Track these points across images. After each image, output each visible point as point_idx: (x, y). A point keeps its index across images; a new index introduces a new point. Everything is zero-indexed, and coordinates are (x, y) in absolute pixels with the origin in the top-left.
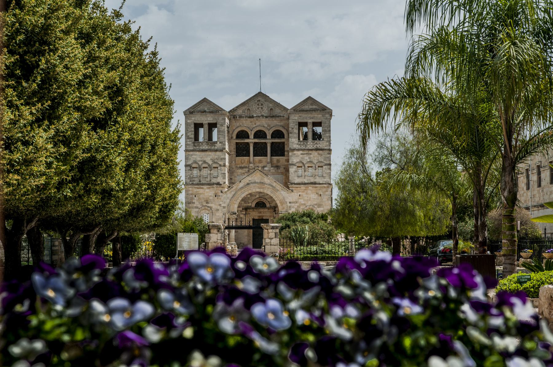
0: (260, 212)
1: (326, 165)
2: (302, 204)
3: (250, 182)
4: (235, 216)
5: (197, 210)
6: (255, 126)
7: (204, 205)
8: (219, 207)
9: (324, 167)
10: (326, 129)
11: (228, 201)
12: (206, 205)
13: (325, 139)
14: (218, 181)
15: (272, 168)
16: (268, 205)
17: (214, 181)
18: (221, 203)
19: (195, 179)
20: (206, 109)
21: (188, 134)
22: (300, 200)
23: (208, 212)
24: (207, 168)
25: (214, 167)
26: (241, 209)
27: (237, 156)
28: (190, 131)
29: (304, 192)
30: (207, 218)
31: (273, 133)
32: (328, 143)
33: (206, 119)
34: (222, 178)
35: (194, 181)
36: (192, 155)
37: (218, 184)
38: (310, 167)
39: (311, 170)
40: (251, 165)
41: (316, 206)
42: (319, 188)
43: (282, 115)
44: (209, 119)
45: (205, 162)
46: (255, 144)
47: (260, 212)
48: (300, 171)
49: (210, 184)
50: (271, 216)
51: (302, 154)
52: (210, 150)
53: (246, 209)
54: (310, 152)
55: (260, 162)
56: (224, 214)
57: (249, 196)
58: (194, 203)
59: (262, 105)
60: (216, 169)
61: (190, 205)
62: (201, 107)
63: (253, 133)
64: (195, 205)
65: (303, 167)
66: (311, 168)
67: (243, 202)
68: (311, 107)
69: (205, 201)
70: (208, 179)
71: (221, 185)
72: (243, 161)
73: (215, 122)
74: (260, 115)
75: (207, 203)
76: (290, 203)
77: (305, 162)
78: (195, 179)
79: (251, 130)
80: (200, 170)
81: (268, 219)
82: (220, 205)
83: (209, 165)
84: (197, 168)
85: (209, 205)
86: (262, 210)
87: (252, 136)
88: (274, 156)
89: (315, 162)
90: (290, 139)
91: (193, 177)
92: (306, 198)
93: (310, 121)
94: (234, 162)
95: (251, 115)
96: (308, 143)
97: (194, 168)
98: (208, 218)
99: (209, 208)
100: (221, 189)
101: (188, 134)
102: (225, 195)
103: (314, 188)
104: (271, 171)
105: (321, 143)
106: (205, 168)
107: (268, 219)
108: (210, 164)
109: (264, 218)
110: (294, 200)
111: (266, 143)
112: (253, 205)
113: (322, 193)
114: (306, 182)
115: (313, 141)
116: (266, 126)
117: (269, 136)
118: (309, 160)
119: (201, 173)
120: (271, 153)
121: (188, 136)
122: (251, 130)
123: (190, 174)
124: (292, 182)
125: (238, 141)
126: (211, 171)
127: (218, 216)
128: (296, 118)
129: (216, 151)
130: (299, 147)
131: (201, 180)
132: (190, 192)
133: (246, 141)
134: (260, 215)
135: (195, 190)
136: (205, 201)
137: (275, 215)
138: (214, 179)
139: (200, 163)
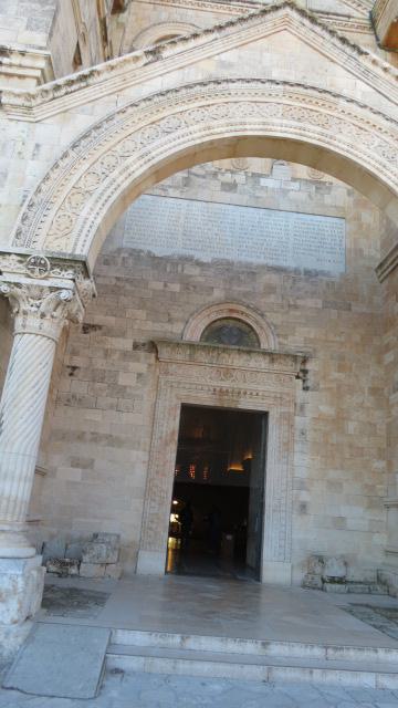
0: (227, 372)
4: (64, 279)
11: (34, 169)
15: (296, 186)
16: (269, 342)
26: (127, 344)
34: (21, 24)
50: (279, 399)
53: (153, 346)
57: (176, 287)
67: (141, 314)
81: (265, 415)
86: (237, 361)
104: (291, 194)
107: (265, 415)
109: (246, 404)
112: (194, 331)
134: (226, 384)
137: (301, 395)
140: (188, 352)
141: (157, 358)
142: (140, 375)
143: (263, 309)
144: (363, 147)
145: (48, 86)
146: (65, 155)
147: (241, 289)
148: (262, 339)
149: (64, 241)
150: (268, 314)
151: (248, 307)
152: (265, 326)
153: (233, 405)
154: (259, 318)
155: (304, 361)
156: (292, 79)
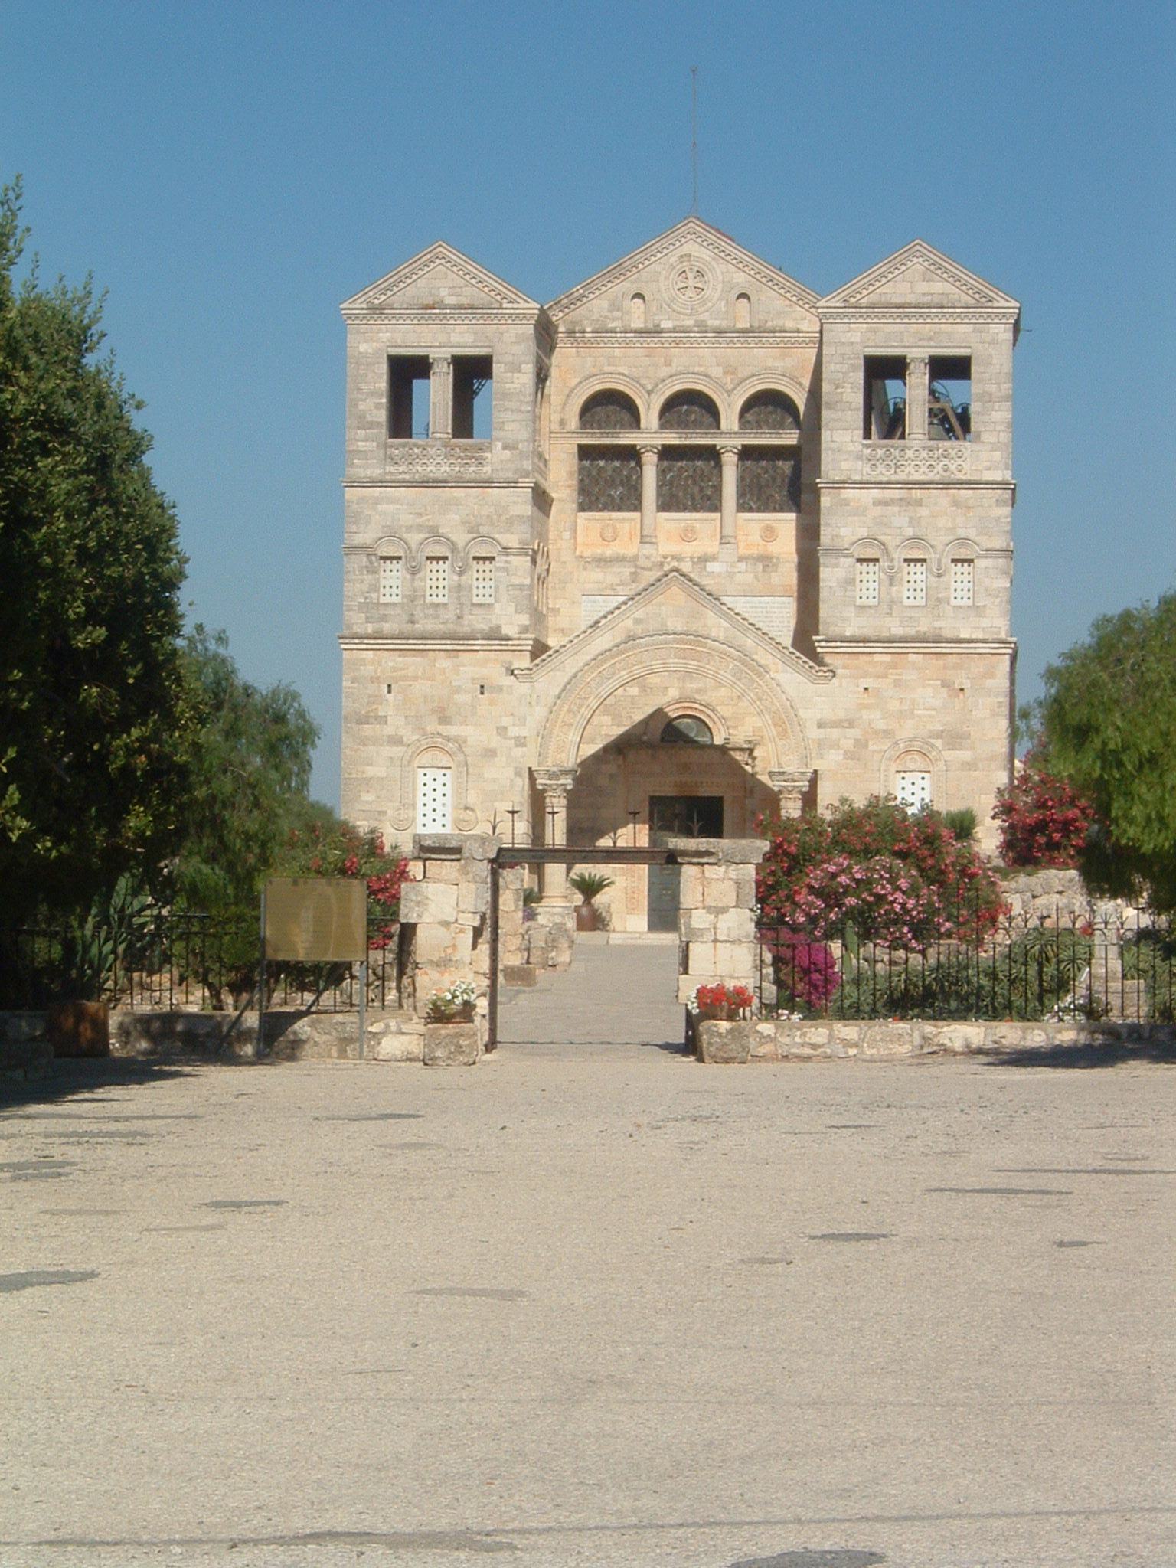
0: (686, 767)
1: (989, 552)
2: (877, 732)
3: (638, 630)
5: (397, 751)
6: (664, 371)
7: (429, 728)
8: (495, 742)
9: (981, 563)
10: (993, 388)
11: (540, 712)
12: (441, 729)
13: (985, 437)
14: (494, 622)
15: (742, 566)
17: (476, 621)
18: (506, 721)
19: (390, 611)
20: (444, 292)
21: (362, 406)
22: (866, 715)
23: (445, 761)
24: (445, 558)
25: (475, 558)
27: (582, 508)
28: (372, 394)
29: (885, 676)
30: (441, 790)
31: (747, 407)
32: (997, 455)
33: (442, 338)
34: (511, 609)
35: (384, 618)
36: (377, 501)
37: (494, 636)
38: (916, 561)
39: (919, 577)
40: (647, 550)
41: (939, 743)
42: (954, 659)
43: (790, 324)
44: (465, 340)
45: (435, 534)
46: (668, 453)
47: (686, 767)
48: (870, 579)
49: (459, 639)
51: (878, 503)
52: (460, 483)
54: (917, 494)
55: (688, 535)
56: (518, 774)
58: (383, 720)
59: (700, 273)
60: (488, 565)
61: (368, 730)
62: (421, 283)
63: (658, 402)
64: (389, 730)
65: (884, 563)
66: (919, 568)
68: (922, 287)
69: (433, 711)
70: (450, 615)
71: (509, 639)
72: (609, 535)
73: (483, 352)
74: (689, 322)
75: (444, 720)
76: (820, 726)
77: (891, 545)
78: (390, 611)
79: (649, 393)
80: (414, 571)
81: (721, 798)
82: (502, 731)
83: (454, 548)
84: (400, 558)
85: (452, 730)
87: (650, 417)
88: (751, 510)
89: (939, 539)
90: (825, 435)
91: (378, 604)
92: (894, 706)
93: (917, 354)
94: (567, 535)
95: (650, 326)
96: (910, 453)
97: (384, 558)
98: (447, 790)
99: (451, 746)
100: (507, 656)
101: (362, 406)
102: (522, 688)
103: (933, 661)
105: (967, 453)
106: (438, 559)
107: (721, 798)
108: (461, 545)
109: (705, 792)
110: (841, 714)
111: (712, 454)
113: (967, 684)
114: (898, 631)
115: (931, 443)
116: (716, 371)
117: (730, 419)
118: (910, 532)
119: (418, 584)
120: (741, 494)
121: (361, 417)
122: (649, 393)
123: (365, 587)
124: (834, 630)
125: (587, 441)
126: (461, 574)
127: (495, 781)
128: (856, 338)
129: (487, 483)
130: (867, 469)
131: (418, 613)
132: (368, 670)
133: (626, 439)
135: (391, 662)
136: (433, 711)
138: (476, 611)
139: (414, 538)
140: (650, 752)
141: (624, 758)
142: (611, 776)
143: (714, 704)
144: (722, 672)
145: (537, 661)
146: (555, 704)
147: (694, 686)
148: (715, 733)
149: (563, 755)
150: (718, 708)
151: (701, 705)
152: (716, 719)
153: (694, 794)
154: (711, 713)
155: (751, 751)
156: (679, 629)
